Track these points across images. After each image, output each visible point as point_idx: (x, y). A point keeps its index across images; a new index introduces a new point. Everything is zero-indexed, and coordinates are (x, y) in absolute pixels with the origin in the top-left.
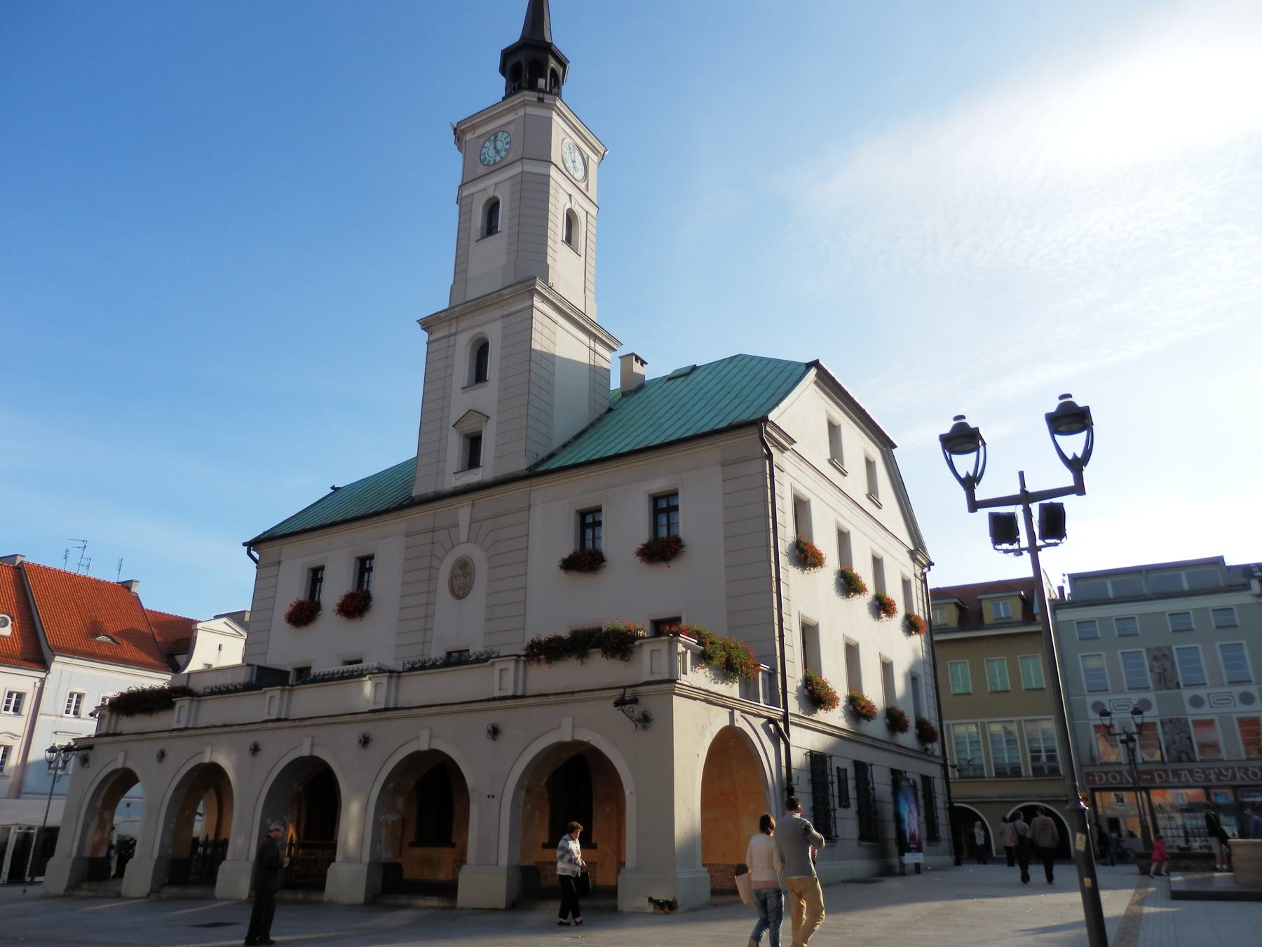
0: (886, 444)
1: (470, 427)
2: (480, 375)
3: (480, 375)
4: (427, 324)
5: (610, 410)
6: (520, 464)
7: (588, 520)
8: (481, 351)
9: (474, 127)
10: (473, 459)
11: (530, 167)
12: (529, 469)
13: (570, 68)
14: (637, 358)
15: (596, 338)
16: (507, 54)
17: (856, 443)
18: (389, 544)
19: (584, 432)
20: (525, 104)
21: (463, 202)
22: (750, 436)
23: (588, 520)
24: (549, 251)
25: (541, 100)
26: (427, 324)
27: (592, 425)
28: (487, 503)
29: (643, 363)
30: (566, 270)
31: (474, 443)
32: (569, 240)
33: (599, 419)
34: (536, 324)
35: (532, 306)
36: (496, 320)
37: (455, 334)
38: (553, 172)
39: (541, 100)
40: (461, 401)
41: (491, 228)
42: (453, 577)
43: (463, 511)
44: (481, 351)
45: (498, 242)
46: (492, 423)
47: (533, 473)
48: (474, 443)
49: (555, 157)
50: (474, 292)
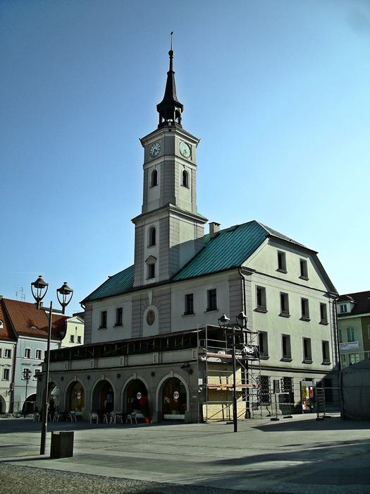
0: (313, 254)
1: (151, 262)
2: (153, 243)
3: (153, 243)
4: (134, 221)
5: (204, 247)
6: (167, 277)
7: (189, 299)
8: (153, 231)
9: (147, 141)
10: (152, 275)
11: (168, 158)
12: (171, 279)
13: (184, 107)
14: (216, 224)
15: (197, 221)
16: (158, 106)
17: (292, 259)
18: (126, 302)
19: (193, 259)
20: (164, 132)
21: (146, 171)
22: (235, 272)
23: (189, 299)
24: (176, 192)
25: (170, 130)
26: (134, 221)
27: (196, 256)
28: (157, 290)
29: (218, 225)
30: (182, 195)
31: (152, 267)
32: (185, 184)
33: (199, 253)
34: (171, 223)
35: (169, 217)
36: (157, 221)
37: (144, 225)
38: (176, 159)
39: (170, 130)
40: (148, 252)
41: (154, 184)
42: (148, 317)
43: (150, 293)
44: (153, 231)
45: (157, 189)
46: (158, 260)
47: (171, 281)
48: (152, 267)
49: (177, 153)
50: (151, 208)
